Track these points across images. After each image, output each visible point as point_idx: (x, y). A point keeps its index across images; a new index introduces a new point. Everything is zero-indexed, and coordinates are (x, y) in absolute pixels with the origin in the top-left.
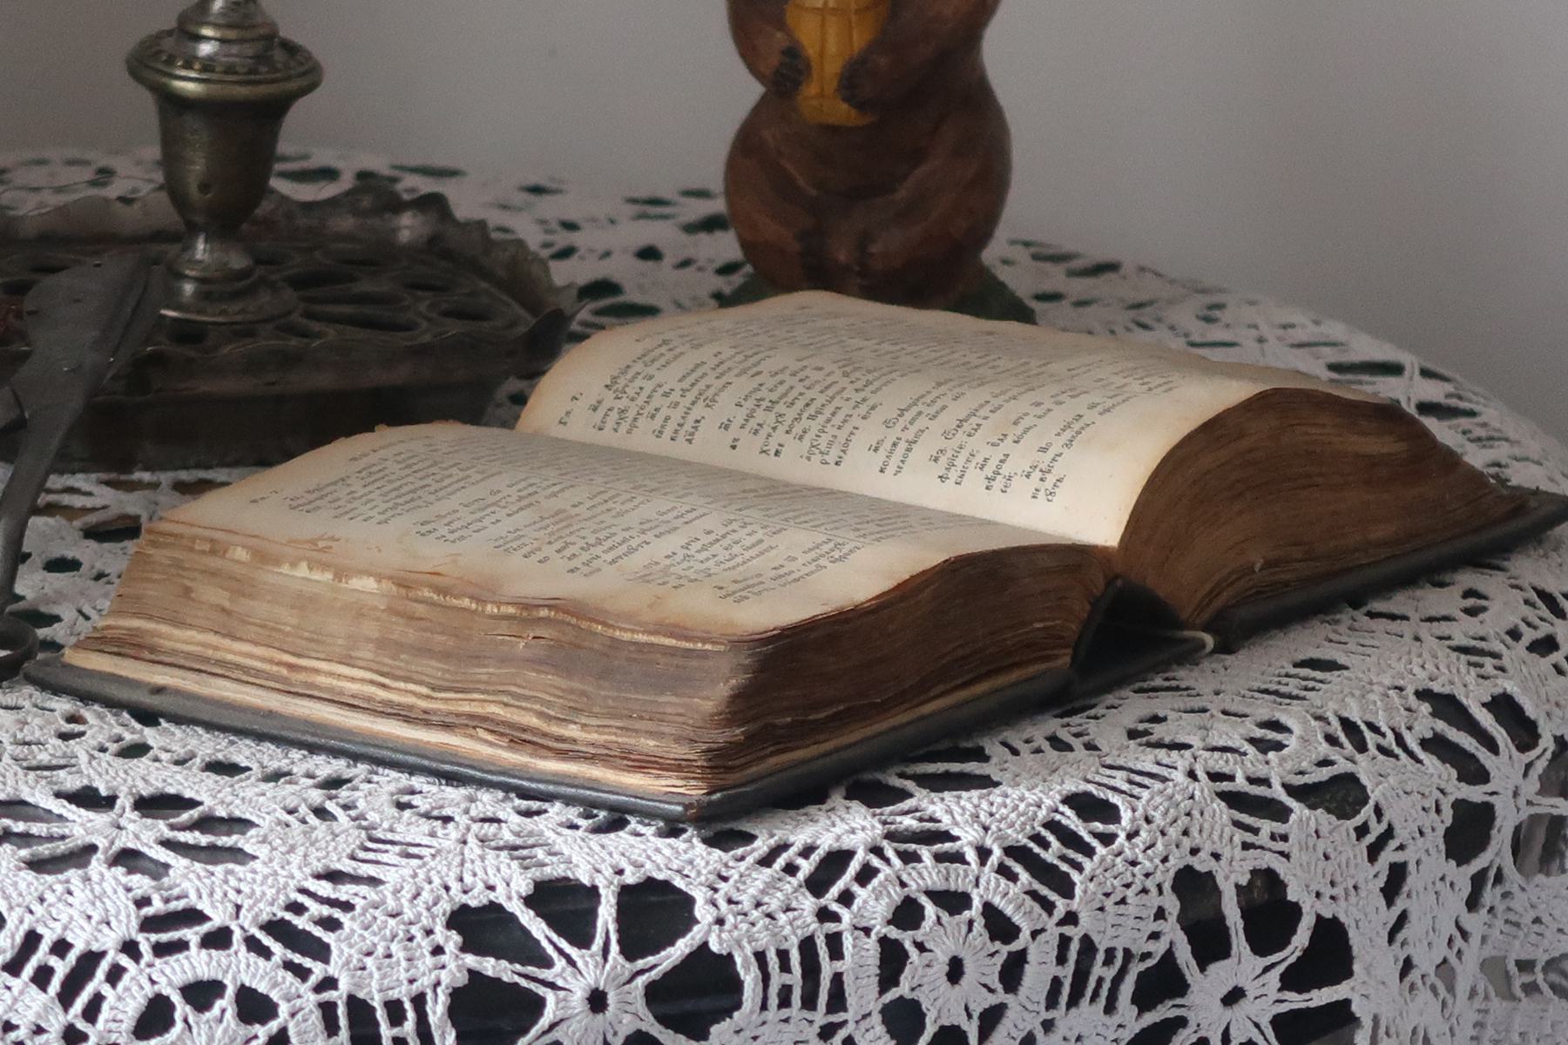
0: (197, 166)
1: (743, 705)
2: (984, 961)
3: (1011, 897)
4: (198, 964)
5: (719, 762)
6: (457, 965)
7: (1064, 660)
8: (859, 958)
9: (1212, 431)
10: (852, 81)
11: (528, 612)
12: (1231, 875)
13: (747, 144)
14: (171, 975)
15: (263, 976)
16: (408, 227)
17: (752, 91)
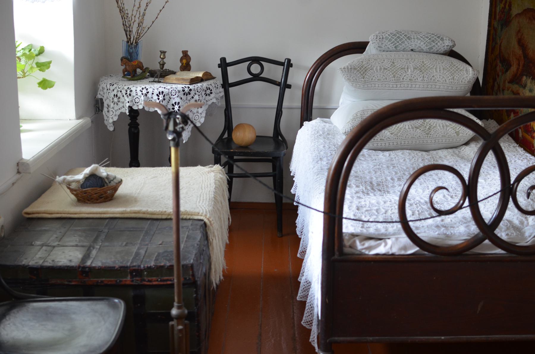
0: (161, 67)
1: (190, 81)
2: (200, 89)
3: (201, 87)
4: (173, 89)
5: (190, 83)
6: (182, 89)
7: (200, 81)
8: (196, 89)
9: (205, 73)
10: (186, 64)
11: (181, 79)
12: (208, 87)
13: (181, 67)
14: (172, 89)
15: (175, 89)
16: (168, 71)
17: (181, 64)
